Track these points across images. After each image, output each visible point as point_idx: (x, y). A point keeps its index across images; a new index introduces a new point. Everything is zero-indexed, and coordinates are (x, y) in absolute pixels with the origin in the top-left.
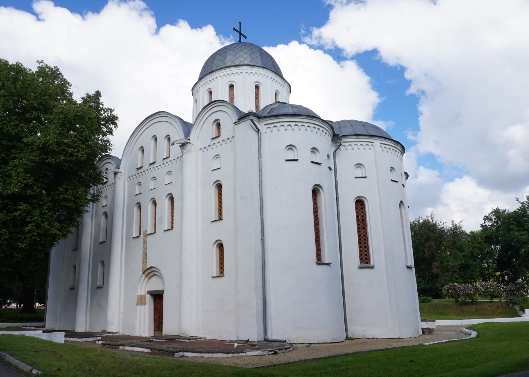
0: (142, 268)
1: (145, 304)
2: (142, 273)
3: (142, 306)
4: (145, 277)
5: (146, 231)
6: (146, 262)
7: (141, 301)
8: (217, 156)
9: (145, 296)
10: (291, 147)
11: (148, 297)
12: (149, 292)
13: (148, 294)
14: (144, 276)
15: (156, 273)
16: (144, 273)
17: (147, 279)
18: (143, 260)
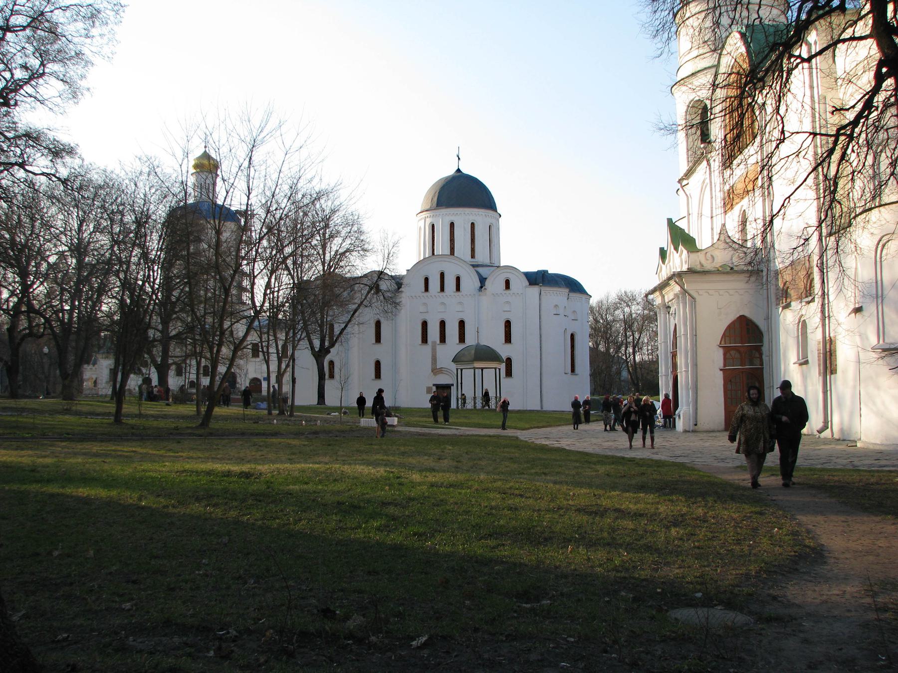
8: (508, 302)
9: (431, 388)
10: (556, 306)
12: (434, 385)
18: (432, 363)
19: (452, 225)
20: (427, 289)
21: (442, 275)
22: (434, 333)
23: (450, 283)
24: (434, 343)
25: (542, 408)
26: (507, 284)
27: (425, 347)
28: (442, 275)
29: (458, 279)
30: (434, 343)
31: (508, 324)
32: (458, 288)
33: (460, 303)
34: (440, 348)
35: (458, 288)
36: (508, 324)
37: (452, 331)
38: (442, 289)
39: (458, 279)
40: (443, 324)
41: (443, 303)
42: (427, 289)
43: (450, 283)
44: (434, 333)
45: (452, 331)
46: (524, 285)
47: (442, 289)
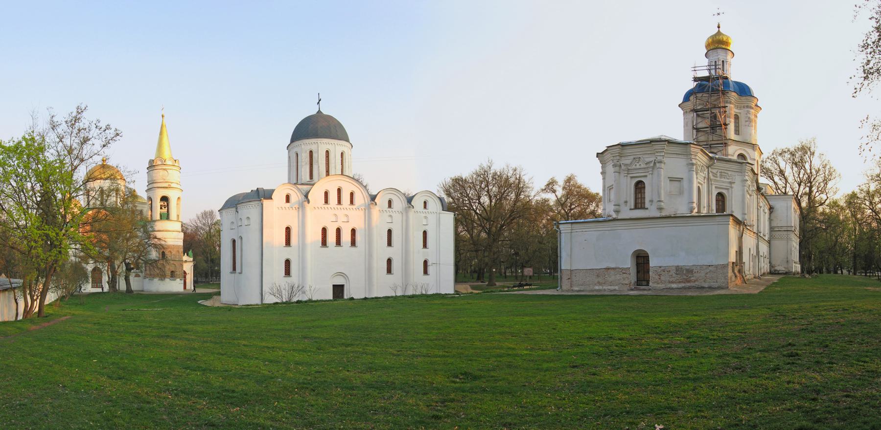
19: (327, 152)
20: (326, 202)
21: (339, 190)
22: (331, 238)
23: (346, 198)
28: (339, 190)
29: (352, 194)
31: (390, 232)
32: (352, 202)
35: (352, 202)
36: (390, 232)
37: (346, 237)
38: (339, 202)
39: (352, 194)
40: (338, 231)
42: (326, 202)
43: (346, 198)
44: (331, 238)
45: (346, 237)
47: (339, 202)
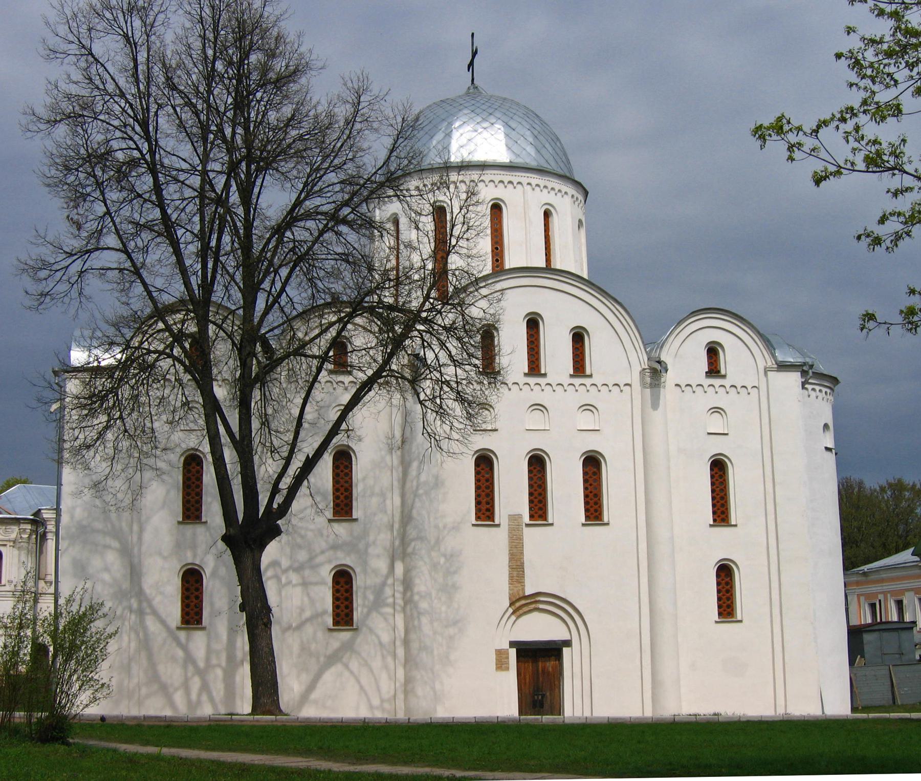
0: (510, 594)
1: (507, 669)
2: (507, 603)
3: (504, 673)
4: (513, 613)
5: (520, 516)
6: (524, 582)
7: (501, 664)
8: (717, 410)
11: (513, 652)
12: (513, 644)
13: (510, 647)
14: (511, 610)
15: (541, 606)
16: (511, 604)
17: (513, 618)
18: (511, 577)
21: (533, 323)
24: (515, 519)
25: (823, 713)
26: (713, 351)
27: (485, 533)
28: (533, 323)
29: (578, 337)
30: (515, 519)
31: (719, 467)
33: (588, 407)
34: (533, 537)
35: (579, 367)
36: (719, 467)
39: (578, 337)
41: (539, 407)
46: (761, 365)
